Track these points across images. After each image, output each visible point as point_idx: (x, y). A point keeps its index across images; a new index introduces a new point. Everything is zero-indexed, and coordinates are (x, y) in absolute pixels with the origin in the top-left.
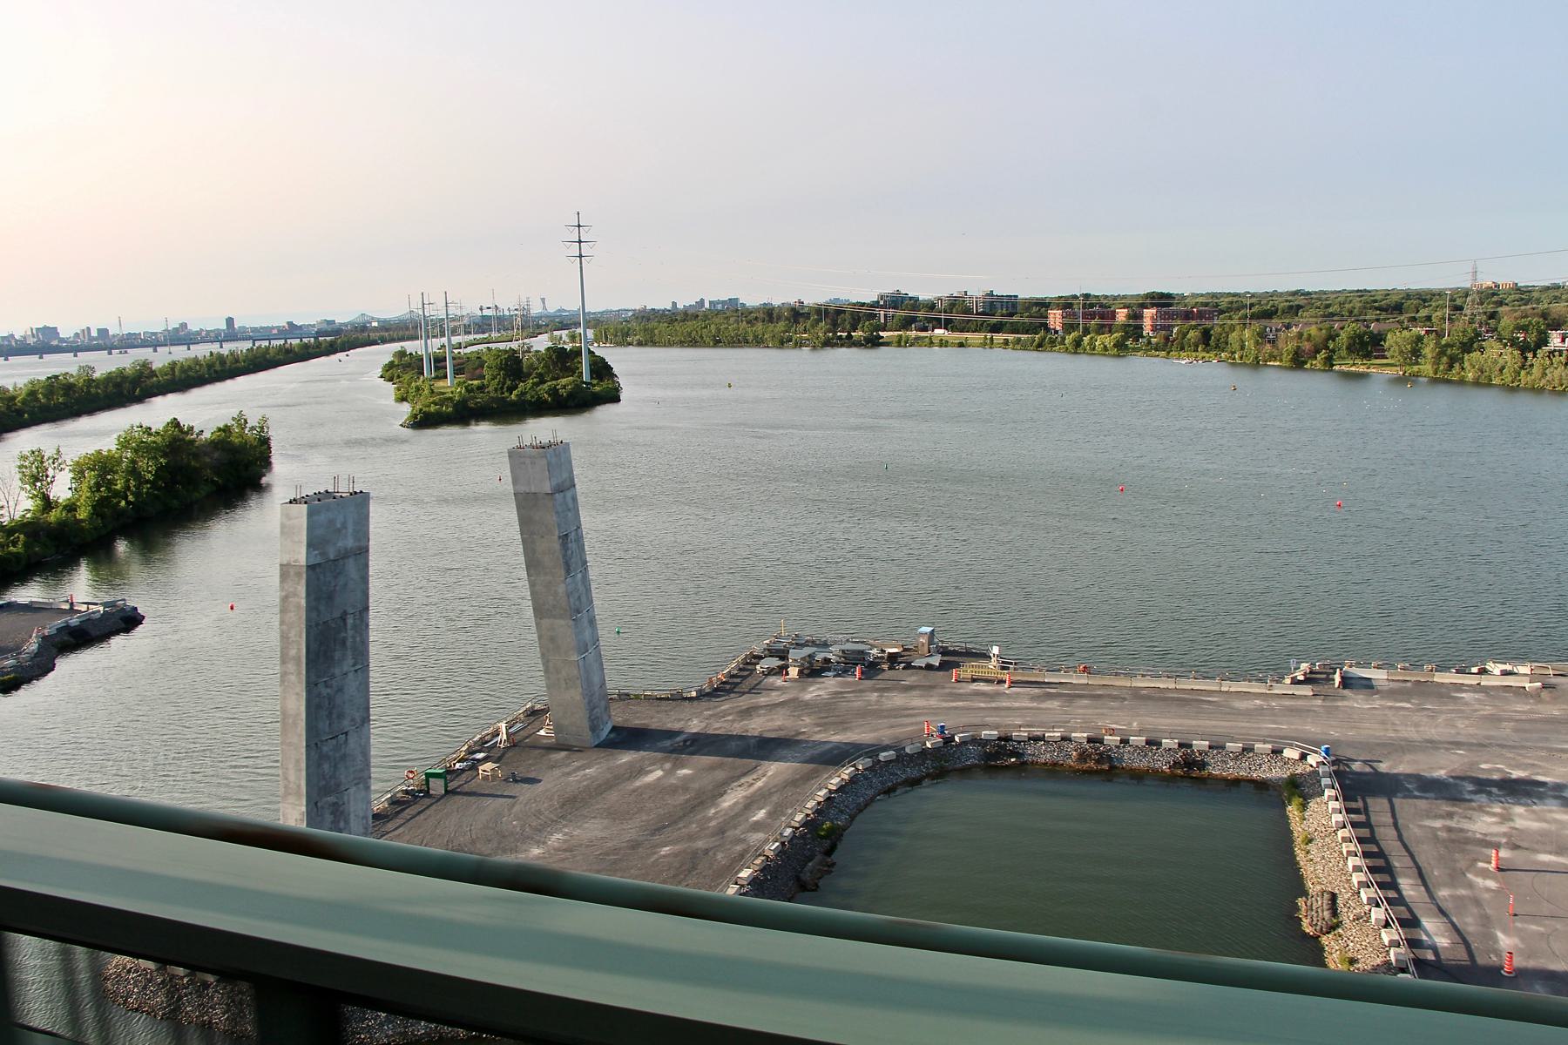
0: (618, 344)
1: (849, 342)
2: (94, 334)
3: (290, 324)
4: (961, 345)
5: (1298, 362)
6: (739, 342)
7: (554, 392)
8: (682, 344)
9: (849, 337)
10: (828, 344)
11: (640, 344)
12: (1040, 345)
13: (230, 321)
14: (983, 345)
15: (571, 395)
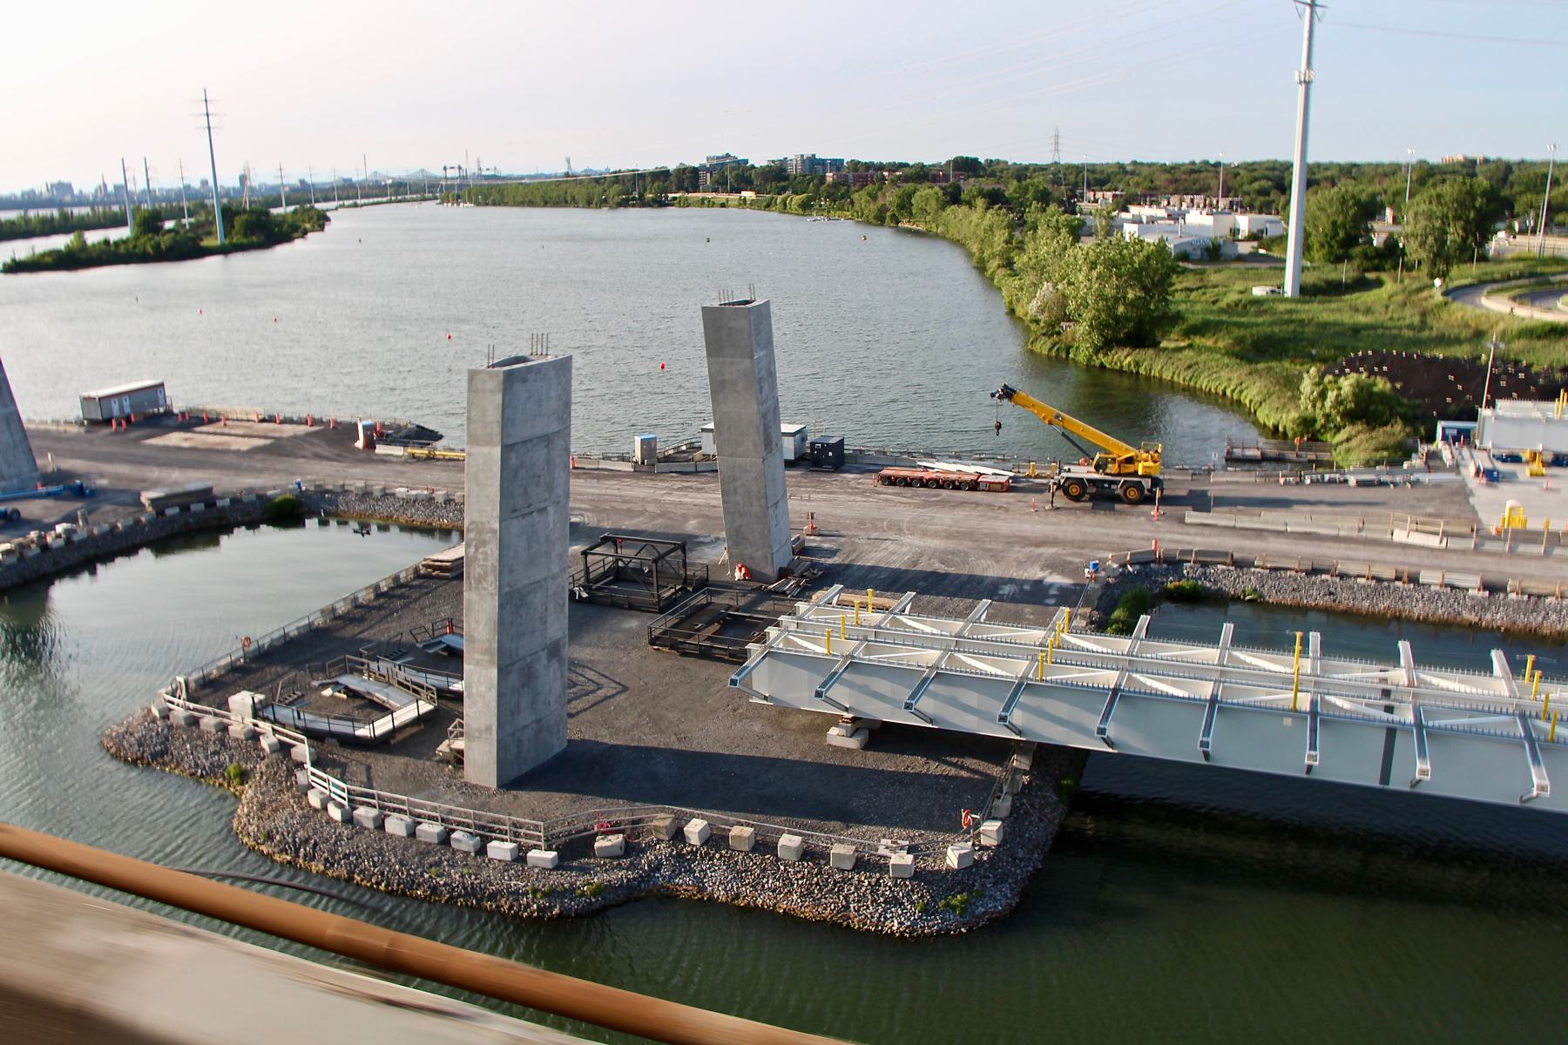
0: (478, 204)
1: (643, 203)
2: (110, 189)
3: (302, 182)
4: (723, 206)
5: (880, 219)
6: (562, 202)
7: (157, 246)
8: (521, 204)
9: (641, 196)
10: (624, 204)
11: (494, 204)
12: (768, 206)
13: (243, 179)
14: (739, 206)
15: (170, 249)
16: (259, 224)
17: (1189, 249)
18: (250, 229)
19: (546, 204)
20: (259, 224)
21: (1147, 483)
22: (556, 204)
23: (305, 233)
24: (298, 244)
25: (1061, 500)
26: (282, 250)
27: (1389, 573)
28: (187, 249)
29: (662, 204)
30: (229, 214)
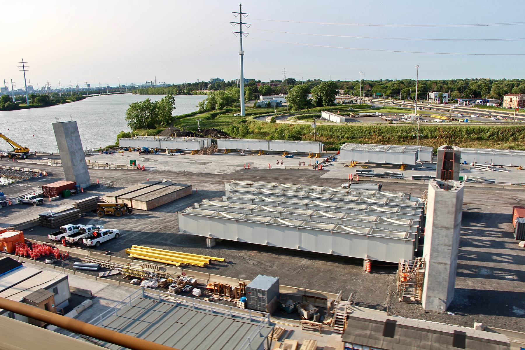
0: (141, 94)
1: (184, 94)
4: (205, 94)
16: (44, 100)
17: (261, 104)
18: (40, 101)
19: (158, 94)
20: (44, 100)
21: (21, 154)
22: (161, 94)
23: (65, 102)
24: (60, 106)
25: (8, 158)
26: (52, 107)
27: (18, 169)
28: (16, 107)
29: (190, 94)
30: (33, 96)
